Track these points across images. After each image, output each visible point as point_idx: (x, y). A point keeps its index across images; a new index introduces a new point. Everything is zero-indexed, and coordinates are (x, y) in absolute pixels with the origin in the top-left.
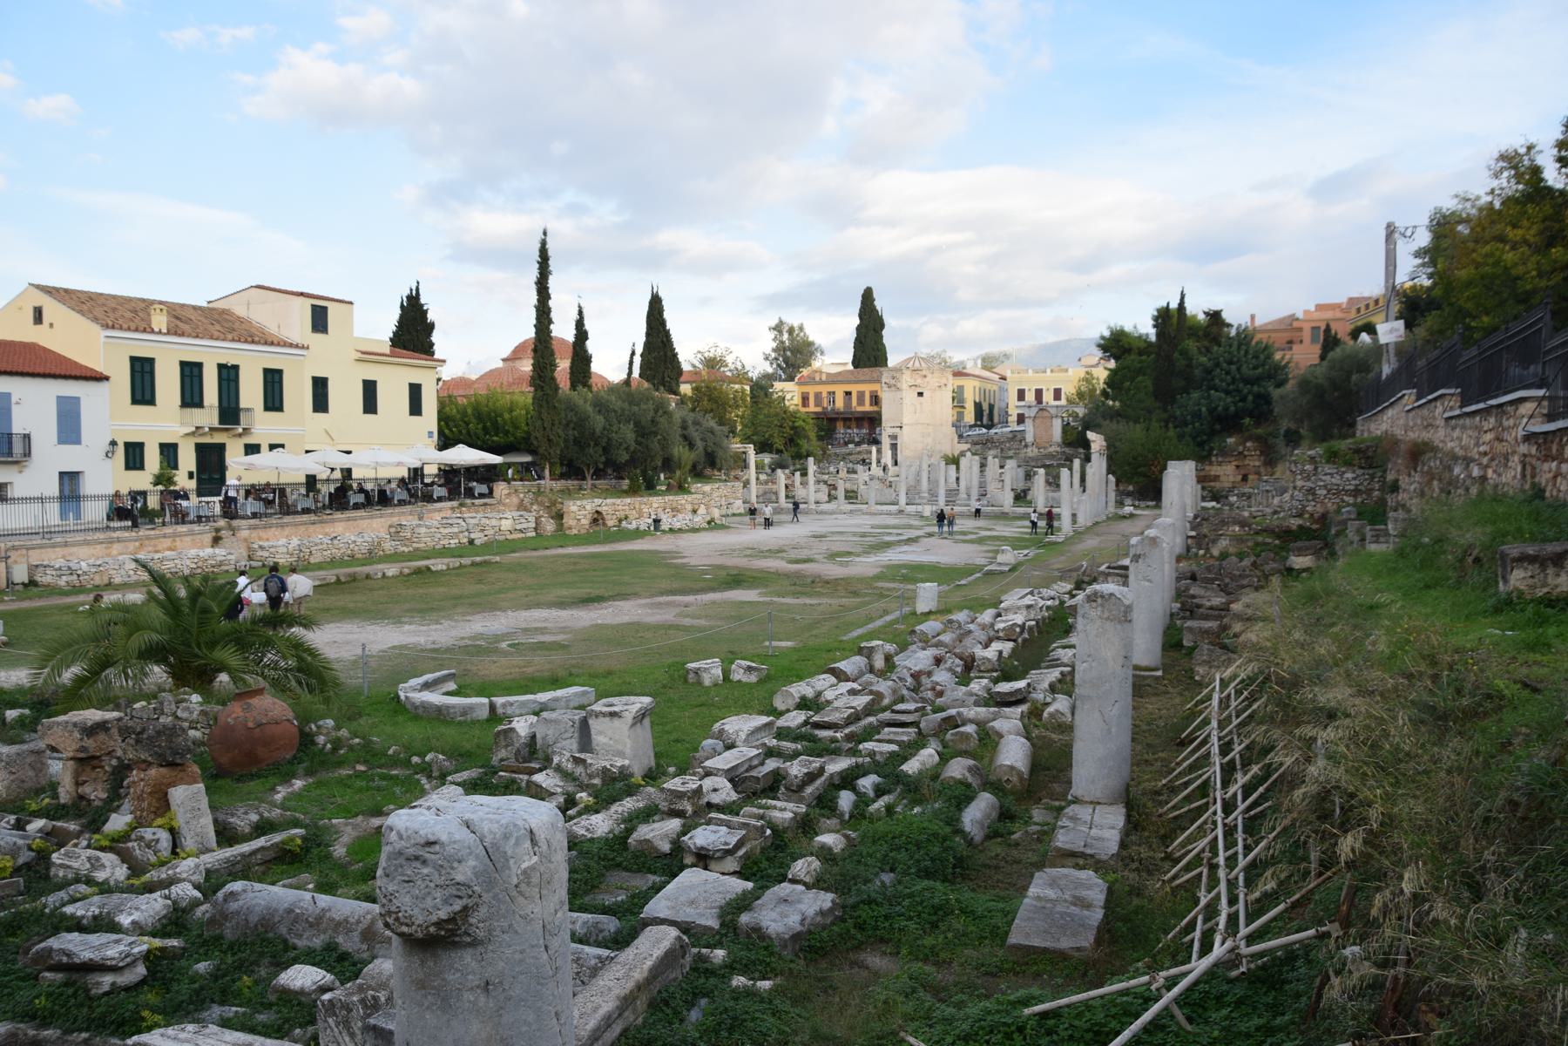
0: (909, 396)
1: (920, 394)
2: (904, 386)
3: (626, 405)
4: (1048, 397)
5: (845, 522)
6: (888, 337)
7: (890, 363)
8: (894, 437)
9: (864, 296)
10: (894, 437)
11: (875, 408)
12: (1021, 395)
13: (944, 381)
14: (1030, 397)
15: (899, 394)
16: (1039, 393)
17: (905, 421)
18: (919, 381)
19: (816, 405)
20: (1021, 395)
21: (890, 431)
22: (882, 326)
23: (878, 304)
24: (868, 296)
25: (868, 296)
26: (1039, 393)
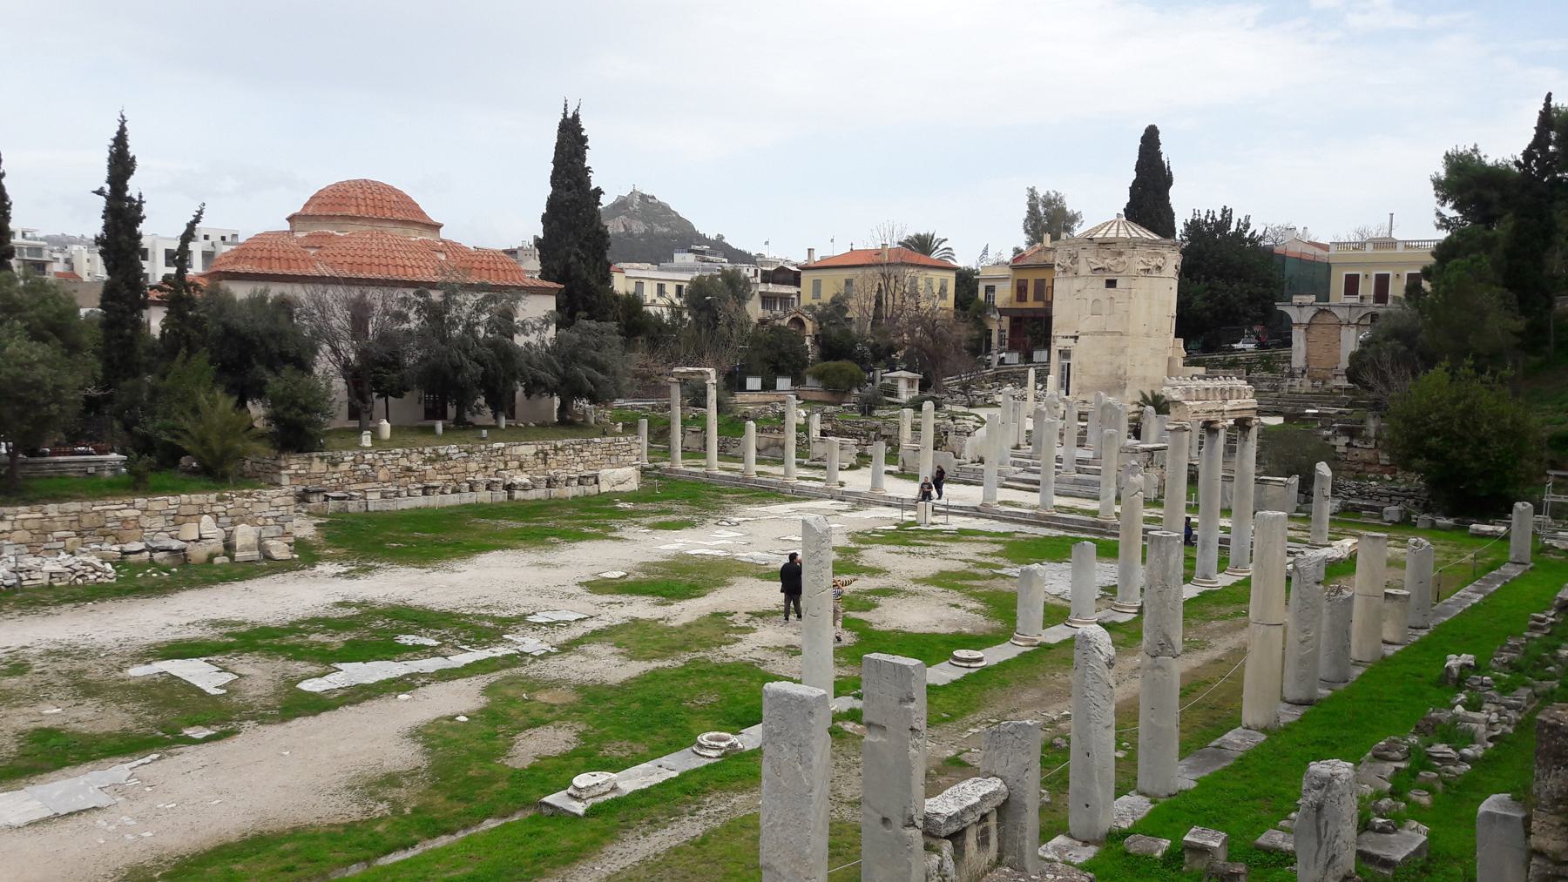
1: (1111, 284)
2: (1083, 268)
3: (312, 304)
5: (536, 577)
8: (1065, 354)
9: (1143, 139)
10: (1065, 354)
11: (1040, 305)
12: (1352, 285)
13: (1159, 261)
14: (1367, 288)
15: (1078, 284)
16: (1382, 281)
19: (1036, 299)
20: (1352, 285)
24: (1150, 139)
25: (1150, 139)
26: (1382, 281)
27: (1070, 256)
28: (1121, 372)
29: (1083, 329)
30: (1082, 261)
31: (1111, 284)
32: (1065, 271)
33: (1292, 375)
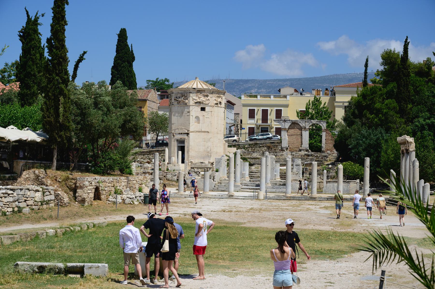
0: (195, 111)
1: (203, 109)
2: (192, 102)
4: (272, 116)
6: (137, 67)
7: (138, 86)
9: (119, 36)
13: (219, 100)
14: (259, 116)
16: (265, 113)
17: (191, 129)
18: (202, 99)
20: (252, 114)
21: (179, 137)
22: (133, 59)
23: (129, 42)
24: (123, 35)
25: (123, 35)
26: (265, 113)
28: (209, 150)
33: (282, 150)
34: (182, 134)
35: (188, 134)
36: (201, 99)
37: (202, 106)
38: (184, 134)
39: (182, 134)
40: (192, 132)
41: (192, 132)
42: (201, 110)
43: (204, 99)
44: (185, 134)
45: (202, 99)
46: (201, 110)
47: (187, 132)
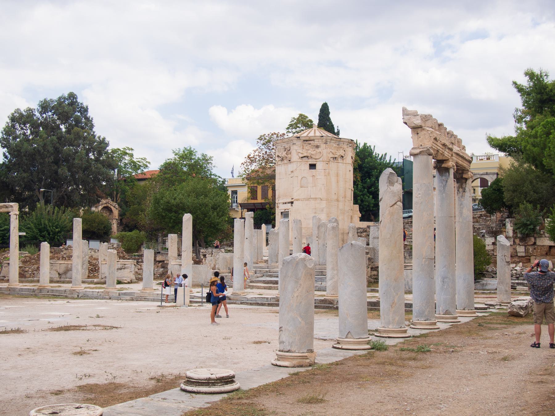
1: (313, 166)
2: (295, 157)
10: (285, 214)
13: (341, 152)
15: (291, 167)
18: (311, 152)
27: (285, 149)
29: (295, 197)
30: (294, 152)
31: (313, 166)
32: (282, 160)
34: (286, 203)
35: (292, 203)
36: (309, 151)
37: (312, 162)
38: (288, 203)
39: (286, 203)
40: (297, 200)
41: (297, 200)
42: (310, 169)
43: (314, 153)
44: (288, 203)
45: (311, 152)
46: (310, 169)
47: (290, 200)
